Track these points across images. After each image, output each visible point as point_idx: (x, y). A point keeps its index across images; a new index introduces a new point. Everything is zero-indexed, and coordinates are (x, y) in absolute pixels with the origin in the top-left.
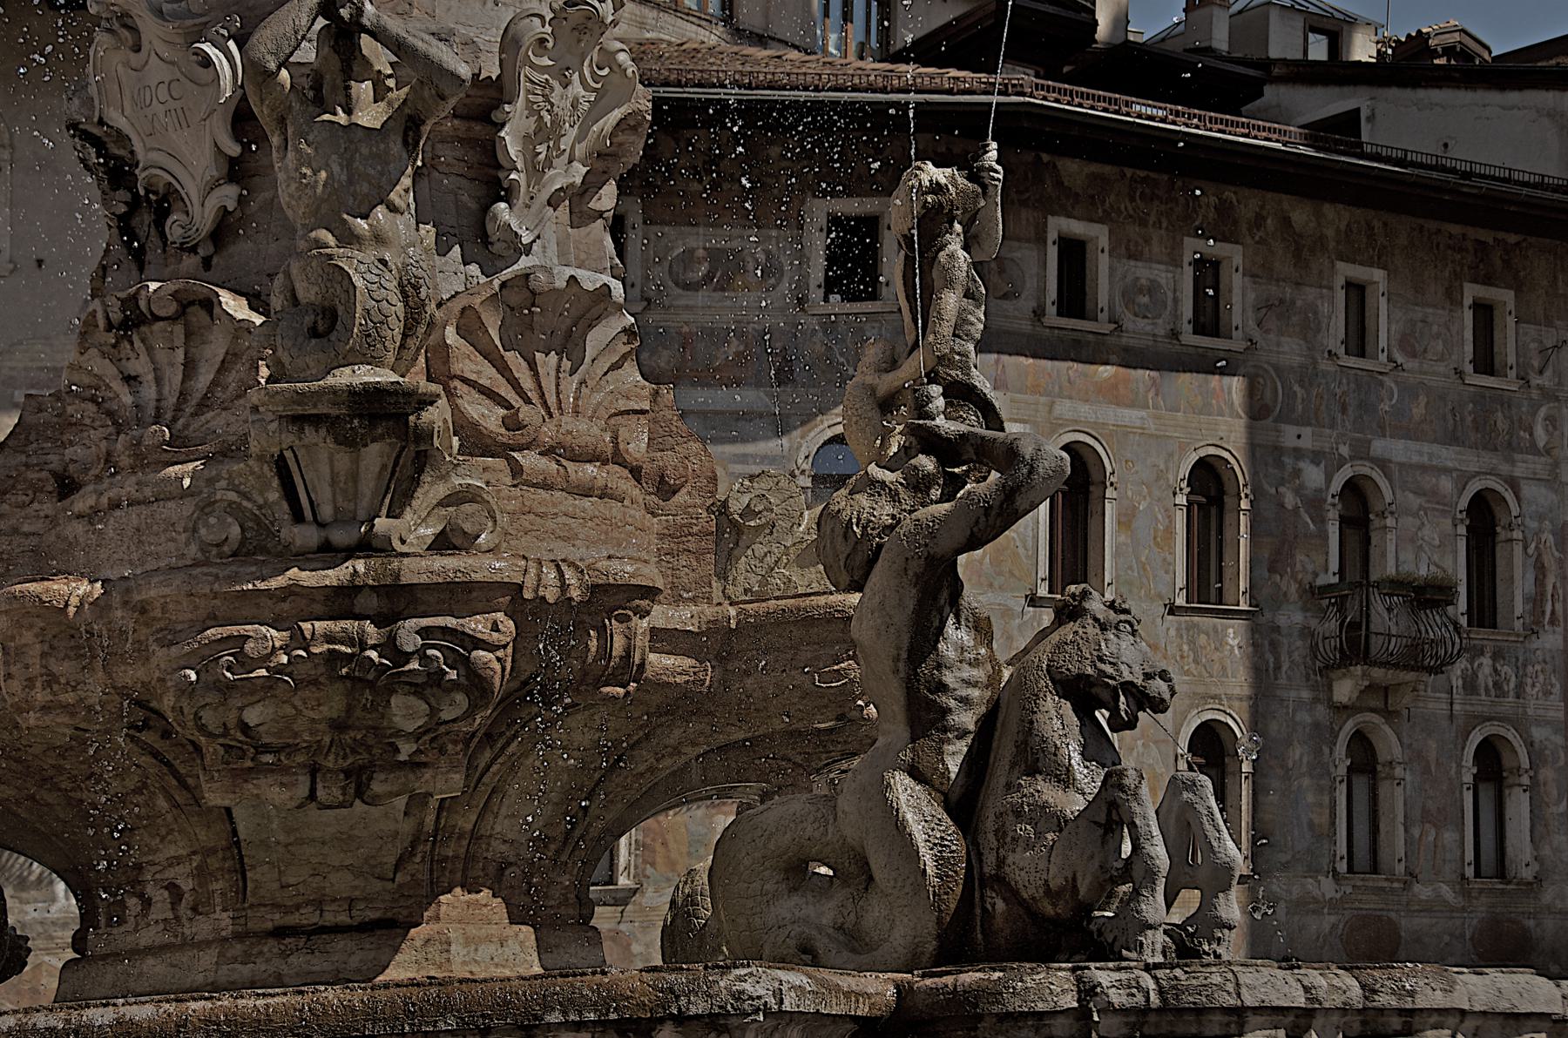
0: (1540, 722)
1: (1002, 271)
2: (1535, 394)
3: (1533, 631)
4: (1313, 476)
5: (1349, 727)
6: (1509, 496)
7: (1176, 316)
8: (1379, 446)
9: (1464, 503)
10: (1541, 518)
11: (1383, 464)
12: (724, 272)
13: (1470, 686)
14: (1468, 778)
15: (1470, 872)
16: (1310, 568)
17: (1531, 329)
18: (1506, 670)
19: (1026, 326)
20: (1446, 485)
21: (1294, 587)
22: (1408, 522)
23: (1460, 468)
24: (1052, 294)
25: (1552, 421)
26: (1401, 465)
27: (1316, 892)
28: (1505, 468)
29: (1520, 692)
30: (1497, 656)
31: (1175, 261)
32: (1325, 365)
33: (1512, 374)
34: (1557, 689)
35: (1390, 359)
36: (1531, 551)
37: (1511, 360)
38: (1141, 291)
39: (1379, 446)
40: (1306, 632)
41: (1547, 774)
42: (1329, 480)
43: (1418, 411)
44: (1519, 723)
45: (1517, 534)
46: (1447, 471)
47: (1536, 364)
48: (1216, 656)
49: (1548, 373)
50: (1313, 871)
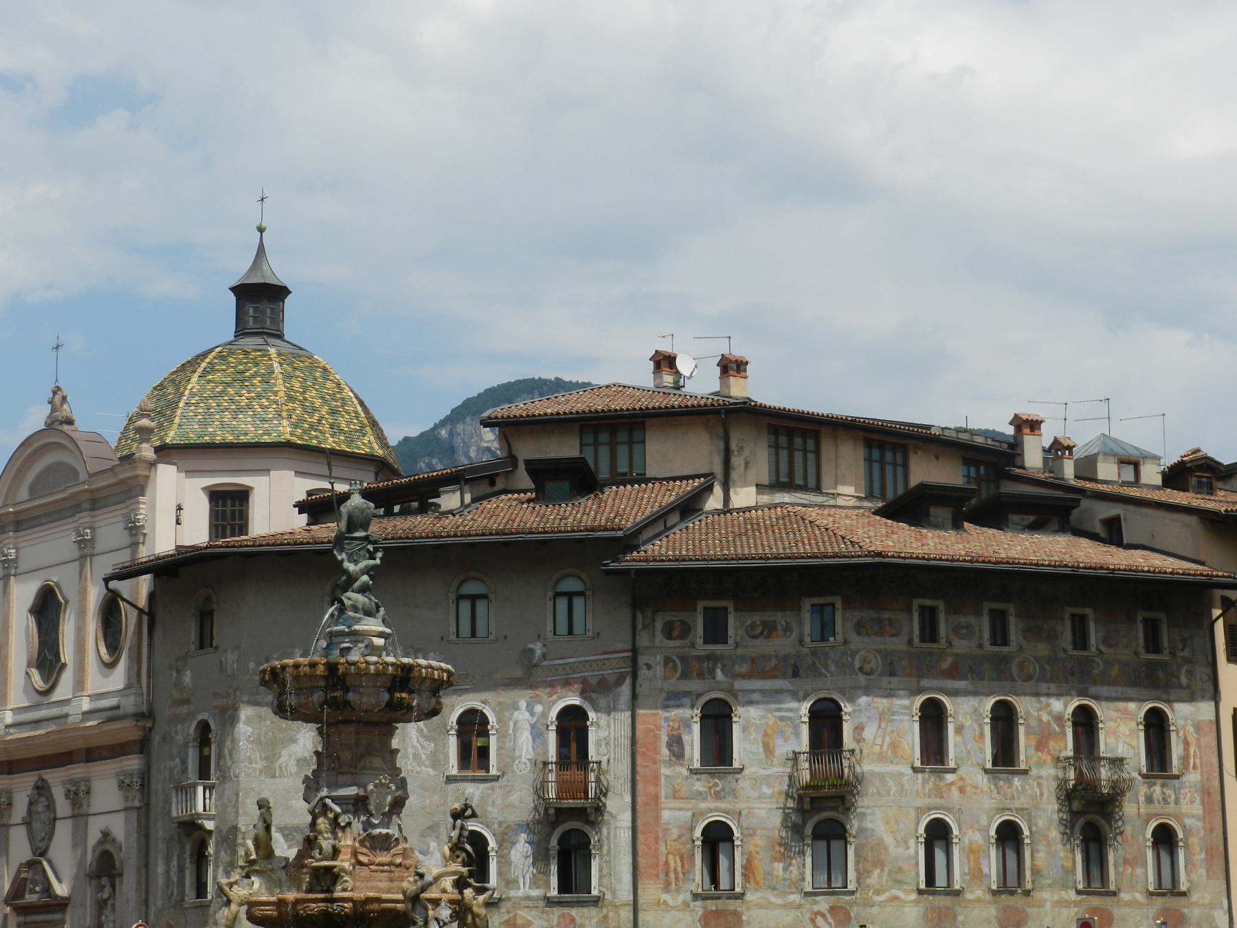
2: (1180, 661)
5: (1081, 822)
7: (981, 638)
12: (769, 630)
18: (1168, 792)
19: (904, 648)
21: (1049, 758)
22: (1112, 724)
25: (1190, 673)
27: (1066, 897)
29: (1177, 802)
31: (978, 613)
32: (1061, 655)
33: (1166, 652)
35: (1098, 649)
36: (1181, 733)
37: (1165, 643)
41: (1193, 840)
42: (1066, 706)
43: (1114, 672)
47: (1180, 646)
49: (1187, 650)
50: (1065, 887)
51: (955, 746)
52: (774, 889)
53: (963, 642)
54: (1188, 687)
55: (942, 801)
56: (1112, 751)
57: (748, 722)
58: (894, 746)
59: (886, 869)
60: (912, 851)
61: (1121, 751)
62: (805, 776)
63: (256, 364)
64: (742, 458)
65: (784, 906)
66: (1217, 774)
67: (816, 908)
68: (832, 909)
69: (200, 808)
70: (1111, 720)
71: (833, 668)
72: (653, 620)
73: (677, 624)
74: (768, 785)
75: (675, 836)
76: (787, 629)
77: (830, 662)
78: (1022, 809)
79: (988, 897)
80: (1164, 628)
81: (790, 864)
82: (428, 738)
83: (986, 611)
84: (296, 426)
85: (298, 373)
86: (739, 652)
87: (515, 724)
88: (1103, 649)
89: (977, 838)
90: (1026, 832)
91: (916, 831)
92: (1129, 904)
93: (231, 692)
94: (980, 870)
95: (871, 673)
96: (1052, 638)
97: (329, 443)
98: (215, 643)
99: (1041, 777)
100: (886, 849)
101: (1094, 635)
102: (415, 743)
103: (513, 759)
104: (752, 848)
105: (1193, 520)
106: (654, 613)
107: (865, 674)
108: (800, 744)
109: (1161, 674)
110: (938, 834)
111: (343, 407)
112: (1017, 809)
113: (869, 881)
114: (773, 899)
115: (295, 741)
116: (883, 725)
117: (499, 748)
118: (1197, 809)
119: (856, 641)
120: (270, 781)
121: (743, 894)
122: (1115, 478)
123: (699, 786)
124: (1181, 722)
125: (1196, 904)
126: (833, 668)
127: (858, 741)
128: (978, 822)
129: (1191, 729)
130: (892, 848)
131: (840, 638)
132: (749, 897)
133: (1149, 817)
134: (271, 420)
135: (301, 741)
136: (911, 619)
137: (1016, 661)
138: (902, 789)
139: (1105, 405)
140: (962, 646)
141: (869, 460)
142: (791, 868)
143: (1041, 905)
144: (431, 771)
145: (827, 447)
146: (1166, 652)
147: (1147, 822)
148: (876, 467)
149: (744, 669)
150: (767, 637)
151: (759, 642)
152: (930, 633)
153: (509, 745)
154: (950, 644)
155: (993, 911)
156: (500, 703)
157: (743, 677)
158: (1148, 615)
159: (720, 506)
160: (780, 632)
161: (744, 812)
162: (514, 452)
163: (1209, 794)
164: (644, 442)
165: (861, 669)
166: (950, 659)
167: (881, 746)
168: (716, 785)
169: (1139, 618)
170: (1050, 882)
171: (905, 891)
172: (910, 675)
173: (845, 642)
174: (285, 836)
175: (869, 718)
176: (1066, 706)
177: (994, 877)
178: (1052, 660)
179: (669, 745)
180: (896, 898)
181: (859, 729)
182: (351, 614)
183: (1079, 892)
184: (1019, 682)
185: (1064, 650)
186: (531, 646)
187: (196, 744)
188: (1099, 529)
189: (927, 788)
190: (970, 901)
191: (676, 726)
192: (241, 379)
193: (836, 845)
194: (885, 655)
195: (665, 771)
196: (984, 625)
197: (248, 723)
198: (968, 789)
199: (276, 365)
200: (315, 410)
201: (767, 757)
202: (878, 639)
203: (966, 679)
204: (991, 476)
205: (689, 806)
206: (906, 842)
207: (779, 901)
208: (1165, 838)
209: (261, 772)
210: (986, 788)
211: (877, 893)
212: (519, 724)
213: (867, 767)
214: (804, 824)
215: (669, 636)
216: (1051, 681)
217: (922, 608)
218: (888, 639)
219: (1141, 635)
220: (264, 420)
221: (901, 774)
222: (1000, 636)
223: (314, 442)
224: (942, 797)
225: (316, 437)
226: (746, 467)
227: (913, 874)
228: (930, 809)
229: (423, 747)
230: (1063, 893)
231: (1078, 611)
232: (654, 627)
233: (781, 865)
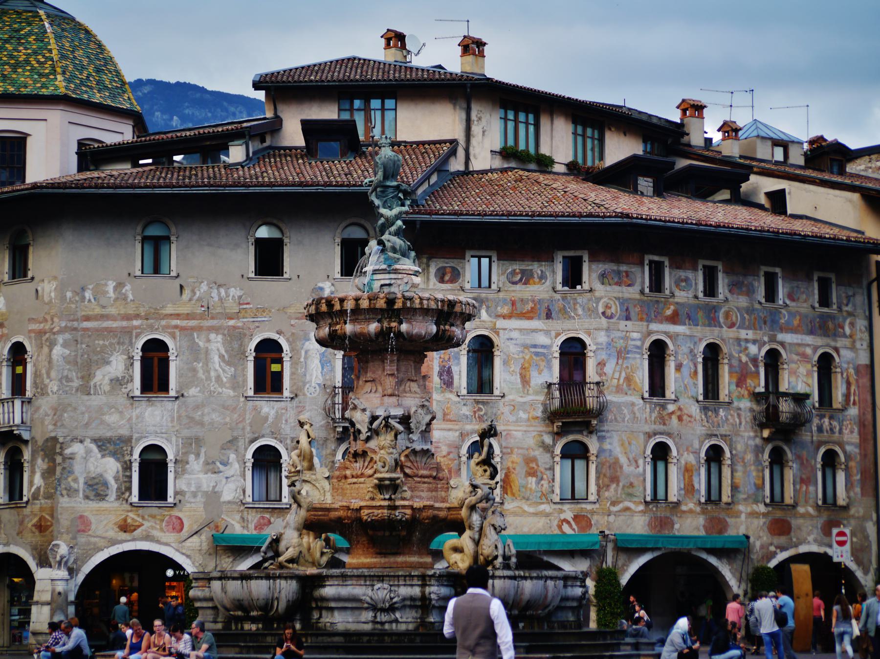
0: (849, 443)
1: (627, 276)
2: (845, 314)
3: (844, 409)
4: (753, 349)
6: (835, 355)
7: (696, 290)
8: (781, 337)
9: (816, 358)
10: (848, 363)
11: (782, 344)
12: (526, 278)
13: (820, 429)
14: (819, 466)
15: (820, 503)
16: (753, 385)
17: (843, 288)
18: (835, 423)
19: (638, 296)
20: (809, 351)
21: (746, 393)
22: (793, 366)
23: (813, 345)
24: (647, 283)
25: (852, 324)
26: (790, 344)
27: (757, 510)
28: (833, 344)
29: (841, 432)
30: (831, 418)
31: (695, 269)
32: (757, 306)
33: (835, 307)
34: (856, 430)
35: (784, 302)
36: (845, 375)
38: (682, 281)
39: (781, 337)
40: (751, 410)
41: (852, 464)
42: (760, 350)
43: (796, 322)
44: (841, 445)
45: (838, 370)
46: (808, 345)
47: (845, 302)
48: (715, 419)
49: (850, 305)
50: (756, 502)
51: (675, 381)
52: (528, 499)
53: (683, 293)
54: (851, 336)
55: (665, 427)
56: (793, 388)
57: (508, 356)
58: (628, 379)
59: (621, 484)
60: (641, 469)
61: (801, 388)
62: (557, 403)
63: (29, 24)
64: (481, 127)
65: (535, 514)
66: (870, 409)
67: (562, 516)
68: (576, 518)
69: (18, 421)
70: (793, 362)
71: (580, 312)
72: (428, 266)
73: (448, 270)
74: (525, 411)
75: (444, 453)
76: (542, 277)
77: (578, 306)
78: (726, 436)
79: (698, 509)
80: (834, 286)
81: (542, 479)
82: (229, 363)
83: (700, 267)
84: (69, 81)
85: (66, 34)
86: (501, 295)
87: (306, 352)
88: (788, 302)
89: (691, 459)
90: (728, 454)
91: (644, 453)
92: (803, 516)
93: (48, 317)
94: (693, 486)
95: (611, 317)
96: (750, 292)
97: (97, 98)
98: (30, 274)
99: (740, 409)
100: (621, 467)
101: (782, 291)
102: (217, 367)
103: (305, 384)
104: (510, 465)
105: (856, 197)
106: (429, 259)
107: (607, 317)
108: (552, 376)
109: (831, 325)
110: (661, 453)
111: (105, 66)
112: (721, 436)
113: (607, 494)
114: (526, 508)
115: (108, 363)
116: (620, 361)
117: (292, 374)
118: (855, 438)
119: (601, 290)
120: (86, 397)
121: (502, 504)
122: (769, 158)
123: (466, 411)
124: (845, 366)
125: (853, 516)
126: (580, 312)
127: (600, 375)
128: (692, 445)
129: (852, 371)
130: (625, 467)
131: (586, 286)
132: (509, 506)
133: (820, 444)
134: (47, 76)
135: (114, 363)
136: (643, 272)
137: (723, 310)
138: (635, 418)
139: (749, 95)
140: (682, 296)
141: (575, 134)
142: (543, 482)
143: (737, 515)
144: (231, 393)
145: (545, 122)
146: (835, 307)
147: (818, 448)
148: (580, 139)
149: (505, 310)
150: (525, 284)
151: (518, 287)
152: (657, 285)
153: (300, 371)
154: (673, 295)
155: (701, 520)
156: (293, 334)
157: (504, 317)
158: (822, 275)
159: (462, 168)
160: (537, 280)
161: (504, 434)
162: (279, 114)
163: (864, 426)
164: (396, 109)
165: (604, 313)
166: (672, 307)
167: (619, 380)
168: (480, 410)
169: (815, 278)
170: (745, 496)
171: (635, 502)
172: (641, 320)
173: (591, 291)
174: (99, 447)
175: (610, 355)
176: (760, 350)
177: (703, 491)
178: (750, 311)
179: (440, 374)
180: (627, 509)
181: (601, 364)
182: (391, 254)
183: (766, 505)
184: (725, 328)
185: (760, 303)
186: (320, 285)
187: (10, 363)
188: (763, 200)
189: (654, 415)
190: (684, 512)
191: (446, 358)
192: (16, 37)
193: (580, 464)
194: (623, 301)
195: (436, 396)
196: (699, 280)
197: (65, 345)
198: (685, 417)
199: (47, 25)
200: (83, 68)
201: (524, 386)
202: (617, 288)
203: (685, 324)
204: (666, 152)
205: (457, 427)
206: (636, 462)
207: (532, 510)
208: (830, 460)
209: (77, 390)
210: (698, 418)
211: (614, 504)
212: (310, 353)
213: (609, 398)
214: (554, 445)
215: (442, 280)
216: (748, 328)
217: (651, 262)
218: (625, 288)
219: (816, 292)
220: (41, 75)
221: (633, 404)
222: (710, 290)
223: (85, 96)
224: (664, 424)
225: (86, 92)
226: (483, 135)
227: (641, 489)
228: (655, 434)
229: (224, 370)
230: (755, 506)
231: (770, 269)
232: (428, 273)
233: (534, 479)
